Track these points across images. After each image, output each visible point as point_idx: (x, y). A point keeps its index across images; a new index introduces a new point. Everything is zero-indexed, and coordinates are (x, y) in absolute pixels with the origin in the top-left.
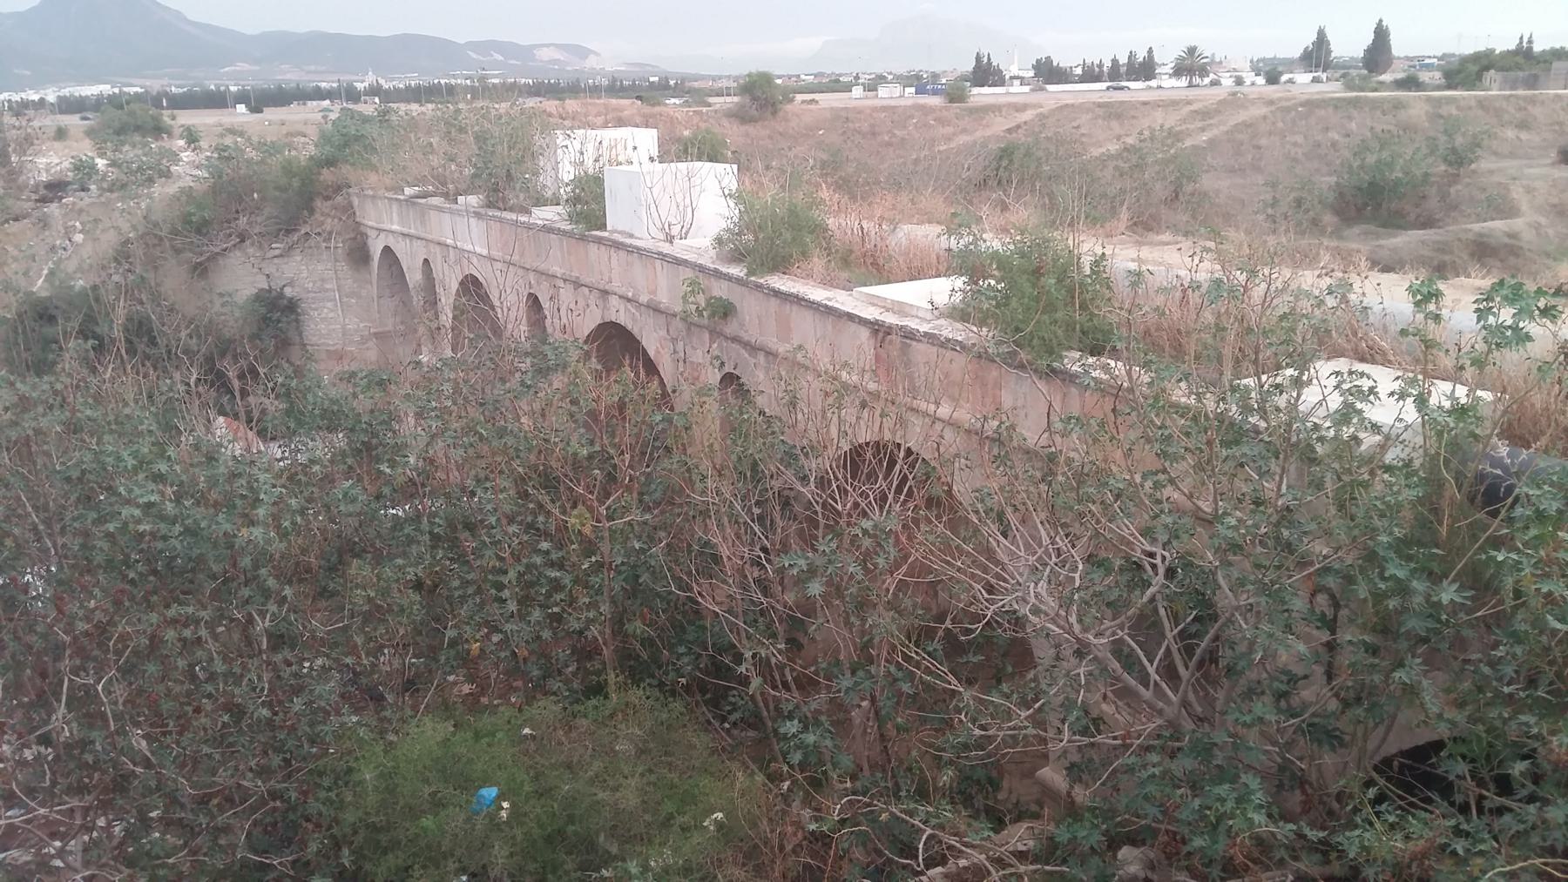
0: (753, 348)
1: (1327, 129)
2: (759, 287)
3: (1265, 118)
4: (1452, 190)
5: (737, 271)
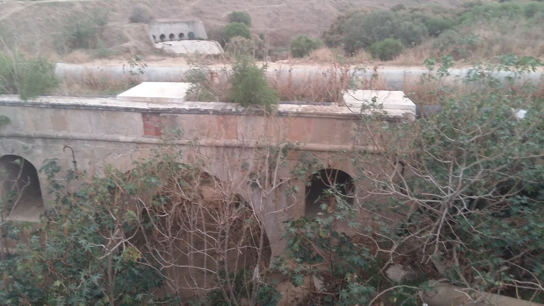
0: (29, 138)
1: (49, 14)
2: (34, 105)
3: (23, 10)
4: (103, 34)
5: (15, 99)
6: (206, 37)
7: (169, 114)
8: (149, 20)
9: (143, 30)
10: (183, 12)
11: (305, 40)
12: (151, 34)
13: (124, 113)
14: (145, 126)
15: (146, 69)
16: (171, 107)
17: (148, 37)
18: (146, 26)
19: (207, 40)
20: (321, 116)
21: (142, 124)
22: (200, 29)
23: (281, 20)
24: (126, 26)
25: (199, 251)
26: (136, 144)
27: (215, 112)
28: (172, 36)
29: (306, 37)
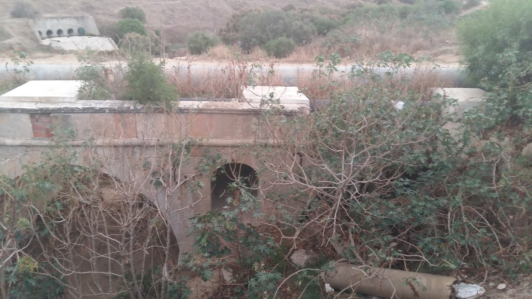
6: (97, 33)
7: (61, 114)
8: (34, 15)
9: (27, 25)
10: (71, 7)
11: (202, 37)
12: (36, 30)
13: (10, 114)
14: (34, 128)
15: (31, 67)
16: (62, 106)
17: (33, 33)
18: (31, 21)
19: (98, 36)
20: (222, 112)
21: (31, 125)
22: (91, 25)
23: (176, 17)
24: (6, 21)
25: (102, 256)
26: (25, 147)
27: (112, 111)
28: (60, 32)
29: (203, 35)
